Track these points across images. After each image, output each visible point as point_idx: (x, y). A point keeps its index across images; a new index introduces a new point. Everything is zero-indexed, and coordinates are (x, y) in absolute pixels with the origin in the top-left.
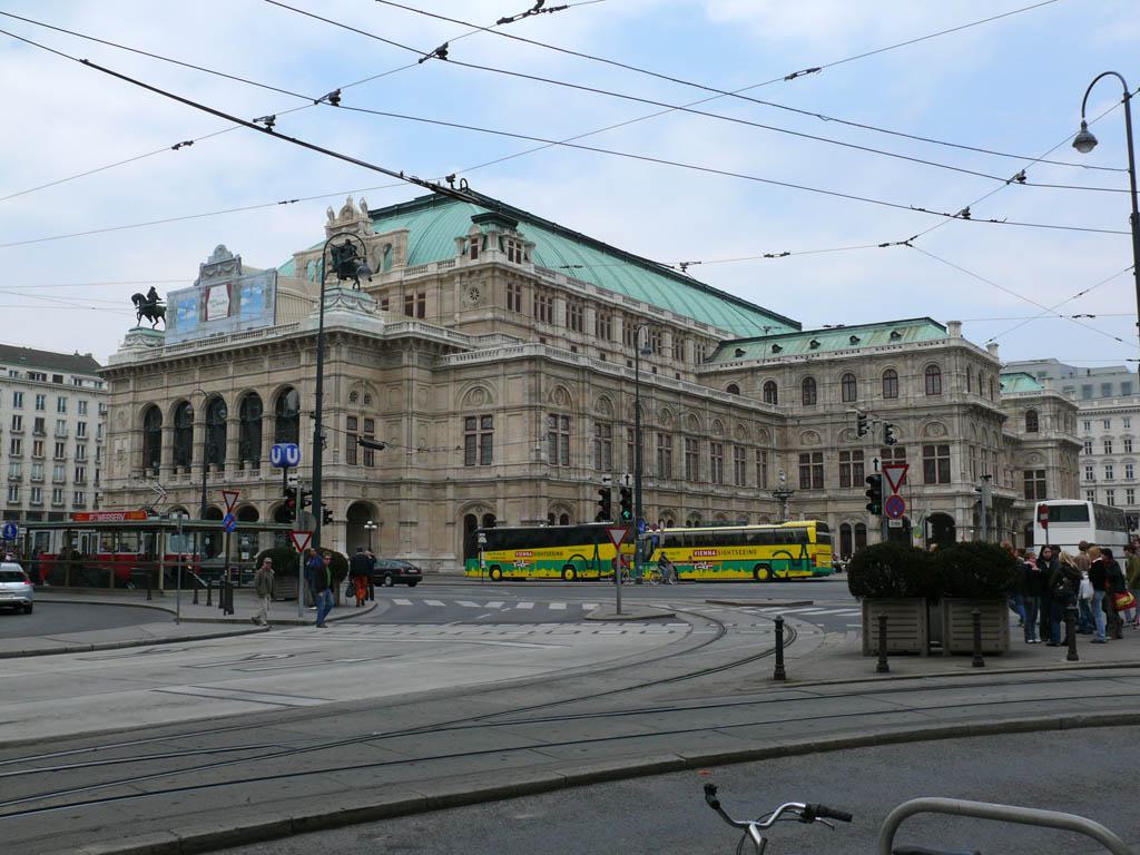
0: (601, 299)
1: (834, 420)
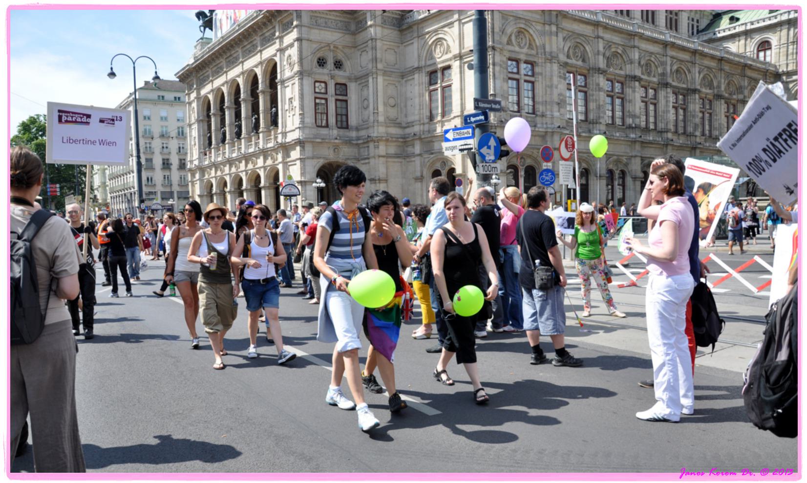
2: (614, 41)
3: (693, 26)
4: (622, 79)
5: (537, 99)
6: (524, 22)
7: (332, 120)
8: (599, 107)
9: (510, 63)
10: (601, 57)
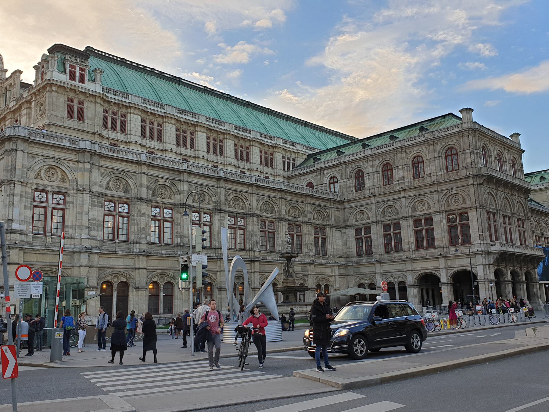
0: (179, 117)
1: (378, 200)
2: (160, 176)
3: (288, 163)
4: (172, 206)
5: (66, 224)
6: (55, 160)
8: (140, 229)
9: (37, 193)
10: (144, 190)
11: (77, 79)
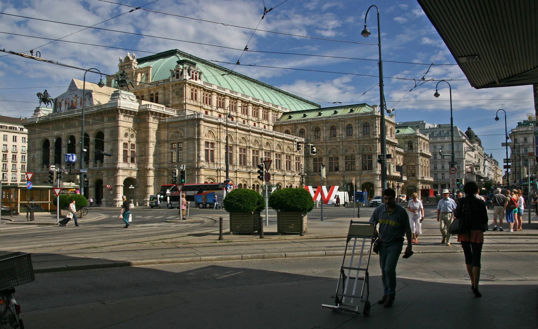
7: (129, 159)
11: (194, 79)
